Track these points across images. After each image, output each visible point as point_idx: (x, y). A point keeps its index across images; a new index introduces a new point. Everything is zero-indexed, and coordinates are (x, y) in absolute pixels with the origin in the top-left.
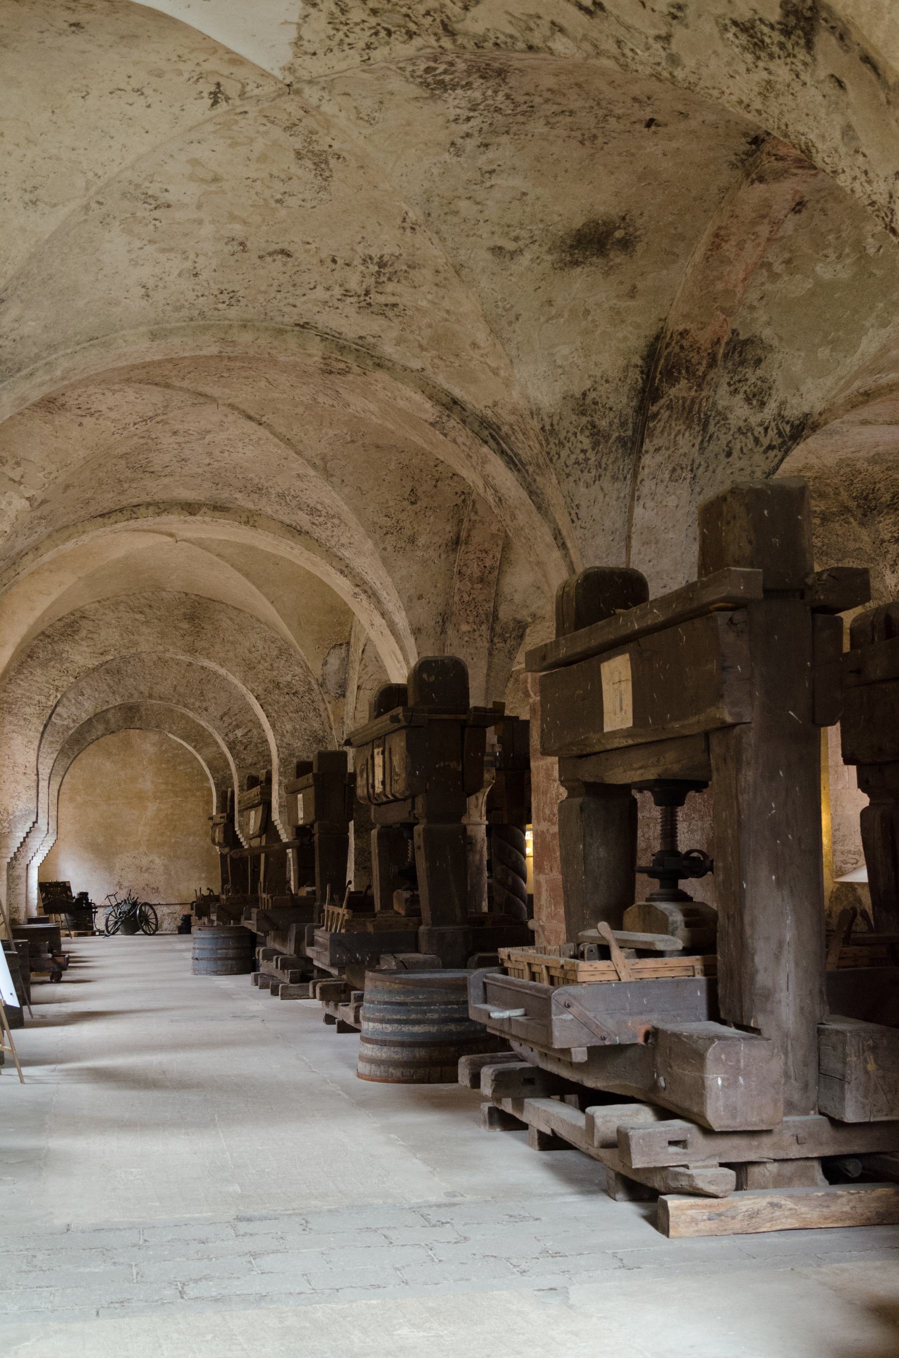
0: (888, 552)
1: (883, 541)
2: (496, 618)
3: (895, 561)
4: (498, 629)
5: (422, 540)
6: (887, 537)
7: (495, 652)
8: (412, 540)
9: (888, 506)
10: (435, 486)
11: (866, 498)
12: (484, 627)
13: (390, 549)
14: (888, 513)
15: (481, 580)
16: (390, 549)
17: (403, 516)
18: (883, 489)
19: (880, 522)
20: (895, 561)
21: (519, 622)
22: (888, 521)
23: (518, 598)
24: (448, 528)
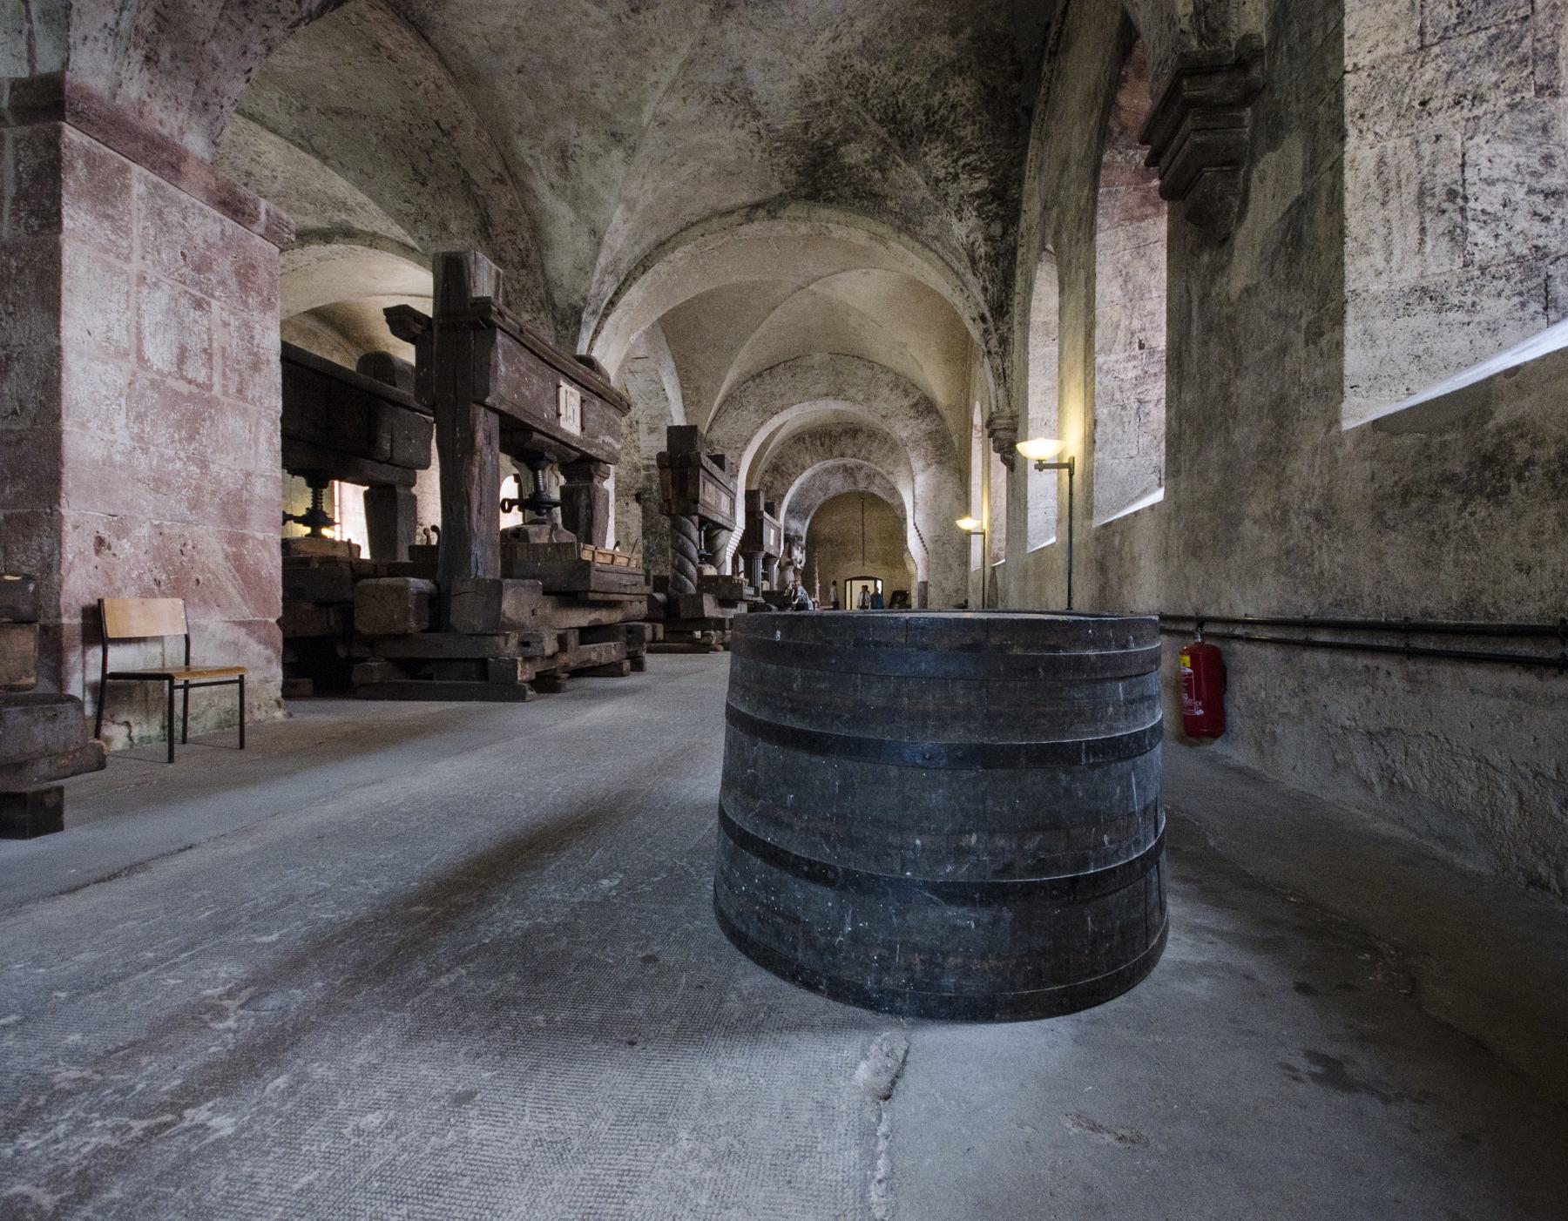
0: (947, 194)
1: (937, 181)
2: (554, 306)
3: (959, 205)
4: (558, 316)
5: (454, 227)
6: (941, 174)
7: (561, 340)
8: (444, 227)
9: (926, 128)
10: (431, 161)
11: (894, 120)
12: (542, 315)
13: (426, 238)
14: (930, 141)
15: (524, 266)
16: (426, 238)
17: (422, 200)
18: (909, 104)
19: (925, 154)
20: (959, 205)
21: (575, 307)
22: (935, 152)
23: (566, 282)
24: (472, 212)
